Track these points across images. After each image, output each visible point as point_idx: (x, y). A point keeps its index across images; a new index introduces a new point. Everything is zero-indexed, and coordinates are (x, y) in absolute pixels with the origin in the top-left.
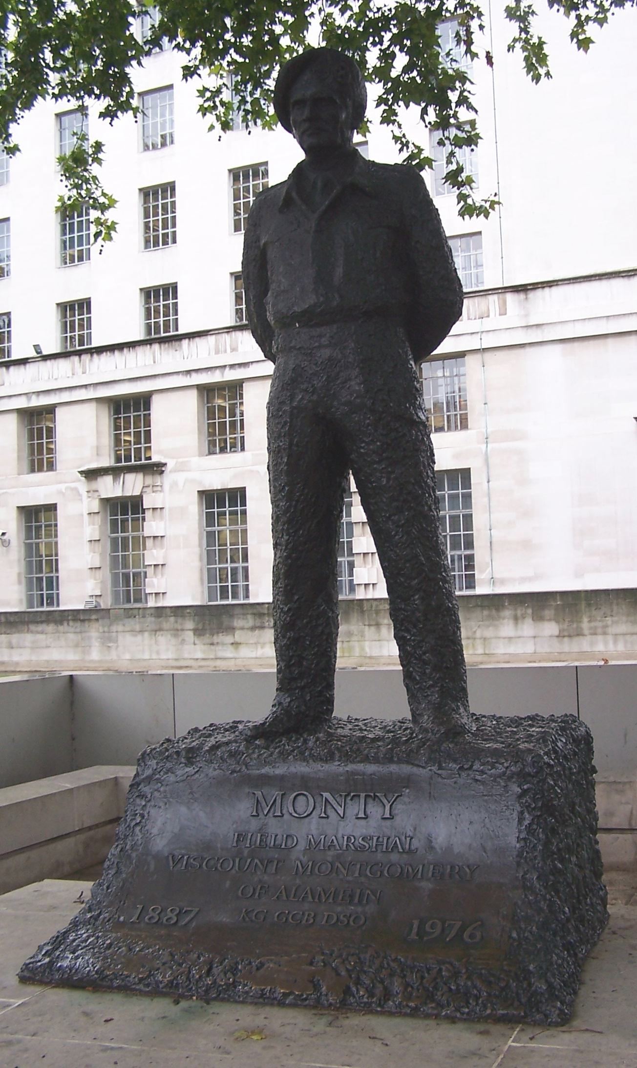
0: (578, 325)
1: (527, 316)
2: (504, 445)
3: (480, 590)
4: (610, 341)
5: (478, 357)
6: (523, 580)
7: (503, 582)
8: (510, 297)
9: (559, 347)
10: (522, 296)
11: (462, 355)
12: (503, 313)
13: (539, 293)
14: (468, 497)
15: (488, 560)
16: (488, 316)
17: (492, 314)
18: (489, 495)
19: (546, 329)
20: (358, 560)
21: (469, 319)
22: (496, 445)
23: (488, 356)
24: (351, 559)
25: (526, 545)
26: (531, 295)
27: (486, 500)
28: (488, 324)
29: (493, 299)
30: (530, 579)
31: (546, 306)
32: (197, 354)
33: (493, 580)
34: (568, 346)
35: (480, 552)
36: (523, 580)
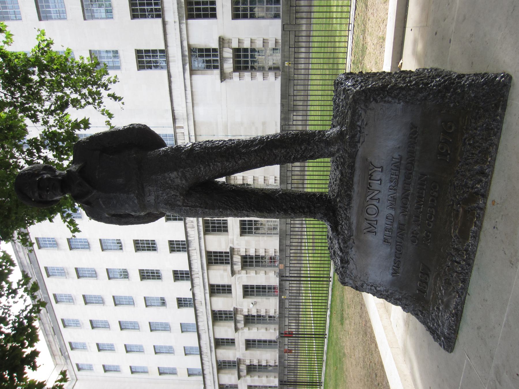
0: (188, 101)
1: (184, 119)
2: (229, 130)
4: (194, 90)
5: (198, 137)
6: (276, 125)
8: (177, 125)
9: (195, 108)
10: (177, 121)
12: (182, 128)
13: (176, 114)
19: (189, 112)
23: (198, 134)
25: (264, 124)
26: (176, 117)
28: (186, 133)
29: (178, 131)
30: (276, 123)
32: (193, 234)
34: (195, 105)
36: (276, 125)
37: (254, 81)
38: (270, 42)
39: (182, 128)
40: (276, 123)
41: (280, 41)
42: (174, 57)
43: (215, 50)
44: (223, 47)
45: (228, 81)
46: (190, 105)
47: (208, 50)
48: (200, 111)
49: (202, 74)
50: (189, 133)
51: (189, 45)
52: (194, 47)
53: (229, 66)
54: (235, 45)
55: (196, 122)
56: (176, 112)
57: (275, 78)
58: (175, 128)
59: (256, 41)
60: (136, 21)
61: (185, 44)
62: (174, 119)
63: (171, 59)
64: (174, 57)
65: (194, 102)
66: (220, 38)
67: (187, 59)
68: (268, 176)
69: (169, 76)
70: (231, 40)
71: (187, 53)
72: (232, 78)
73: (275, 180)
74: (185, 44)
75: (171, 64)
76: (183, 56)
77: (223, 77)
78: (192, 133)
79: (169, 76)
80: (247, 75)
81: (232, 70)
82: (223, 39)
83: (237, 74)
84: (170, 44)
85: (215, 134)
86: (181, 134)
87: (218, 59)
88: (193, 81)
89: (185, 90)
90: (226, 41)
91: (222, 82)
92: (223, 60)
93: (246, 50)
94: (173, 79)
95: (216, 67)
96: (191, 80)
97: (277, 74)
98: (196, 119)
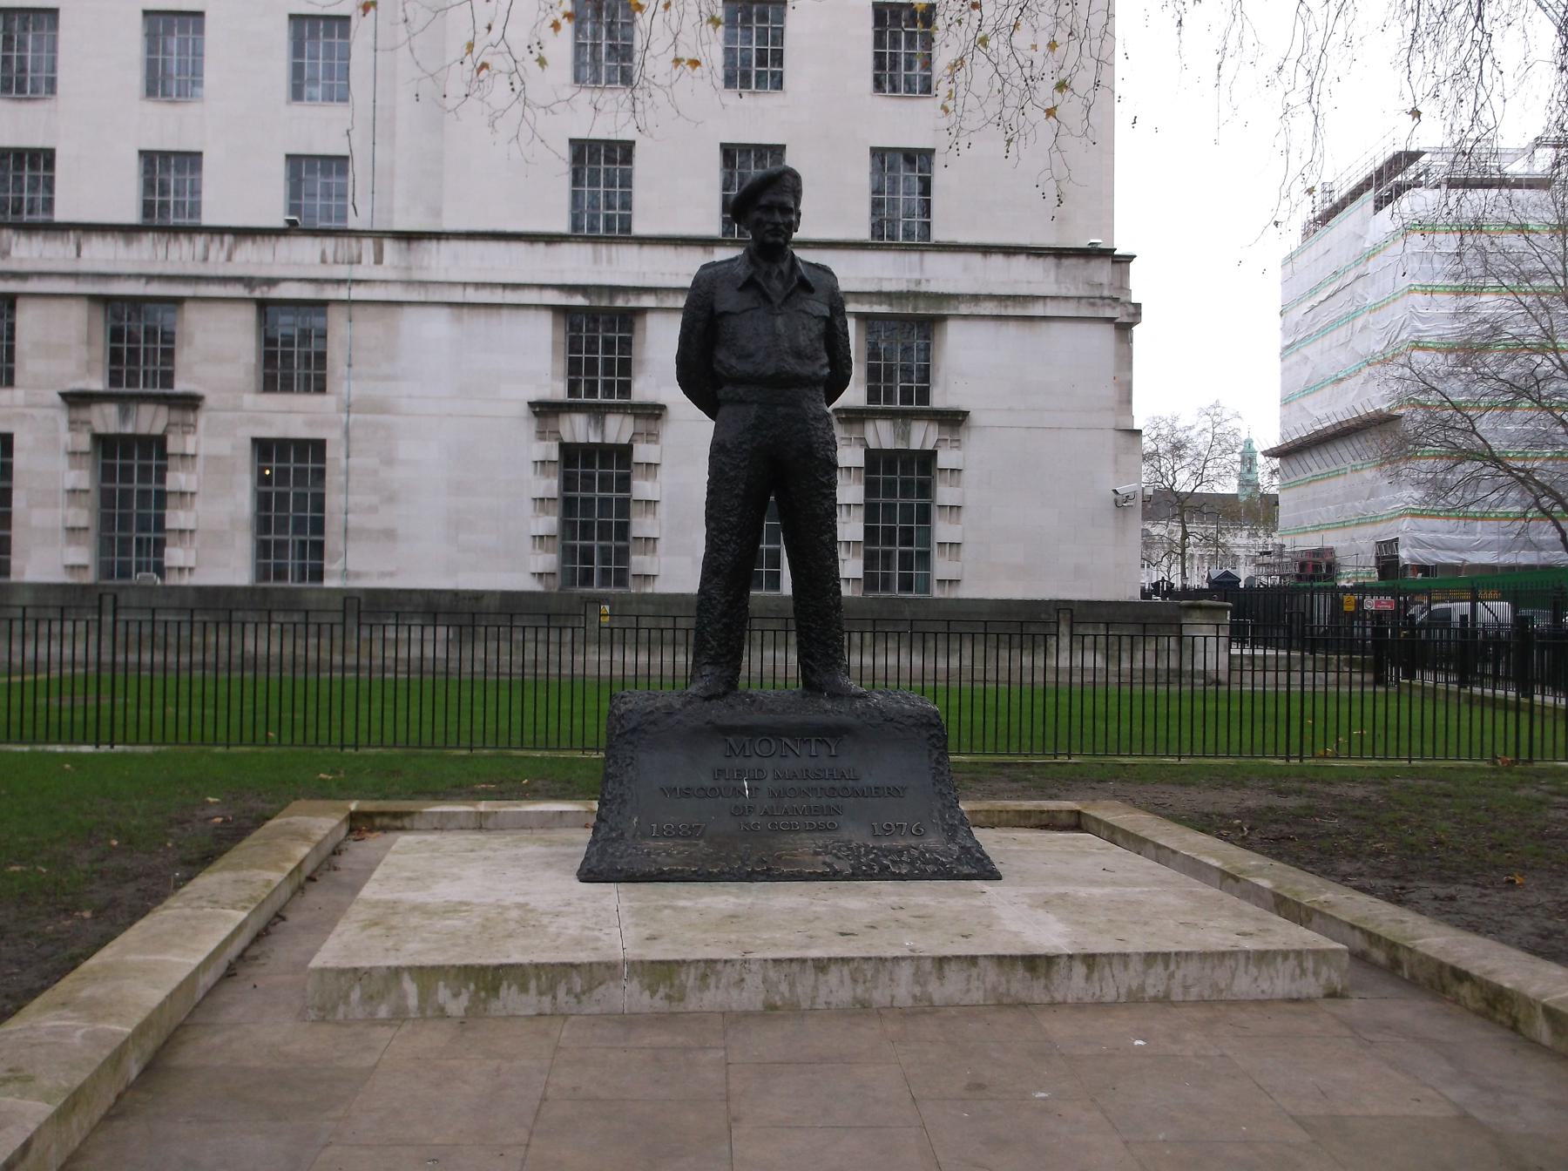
1: (408, 269)
2: (369, 417)
3: (330, 583)
4: (505, 312)
6: (383, 575)
7: (358, 575)
8: (389, 246)
9: (445, 313)
10: (403, 245)
11: (324, 304)
12: (379, 260)
14: (320, 474)
15: (341, 548)
16: (359, 262)
17: (365, 260)
18: (347, 473)
19: (431, 288)
20: (170, 539)
21: (336, 262)
22: (360, 417)
23: (357, 310)
24: (159, 535)
25: (389, 535)
26: (415, 245)
27: (343, 478)
28: (359, 272)
29: (368, 245)
30: (391, 574)
31: (441, 261)
33: (345, 573)
34: (456, 311)
35: (332, 540)
36: (383, 575)
37: (529, 507)
38: (647, 558)
39: (379, 260)
40: (391, 574)
41: (649, 590)
42: (609, 261)
43: (626, 388)
44: (636, 416)
45: (533, 424)
46: (457, 295)
47: (626, 367)
48: (438, 325)
49: (554, 343)
50: (358, 282)
51: (643, 311)
52: (638, 326)
53: (578, 429)
54: (642, 452)
55: (398, 309)
56: (432, 246)
57: (540, 575)
58: (379, 235)
59: (650, 517)
60: (716, 157)
61: (648, 301)
62: (409, 237)
63: (603, 249)
64: (609, 261)
65: (465, 310)
66: (663, 407)
67: (604, 303)
68: (196, 544)
69: (551, 239)
70: (656, 442)
71: (620, 302)
72: (542, 439)
73: (181, 569)
74: (648, 301)
75: (586, 250)
76: (614, 290)
77: (544, 411)
78: (359, 293)
79: (551, 239)
80: (550, 485)
81: (567, 439)
82: (658, 417)
83: (555, 455)
84: (648, 252)
85: (355, 369)
86: (355, 252)
87: (599, 399)
88: (532, 313)
89: (505, 286)
90: (651, 425)
91: (531, 404)
92: (598, 413)
93: (625, 483)
94: (540, 248)
95: (573, 389)
96: (537, 307)
97: (551, 580)
98: (408, 310)
